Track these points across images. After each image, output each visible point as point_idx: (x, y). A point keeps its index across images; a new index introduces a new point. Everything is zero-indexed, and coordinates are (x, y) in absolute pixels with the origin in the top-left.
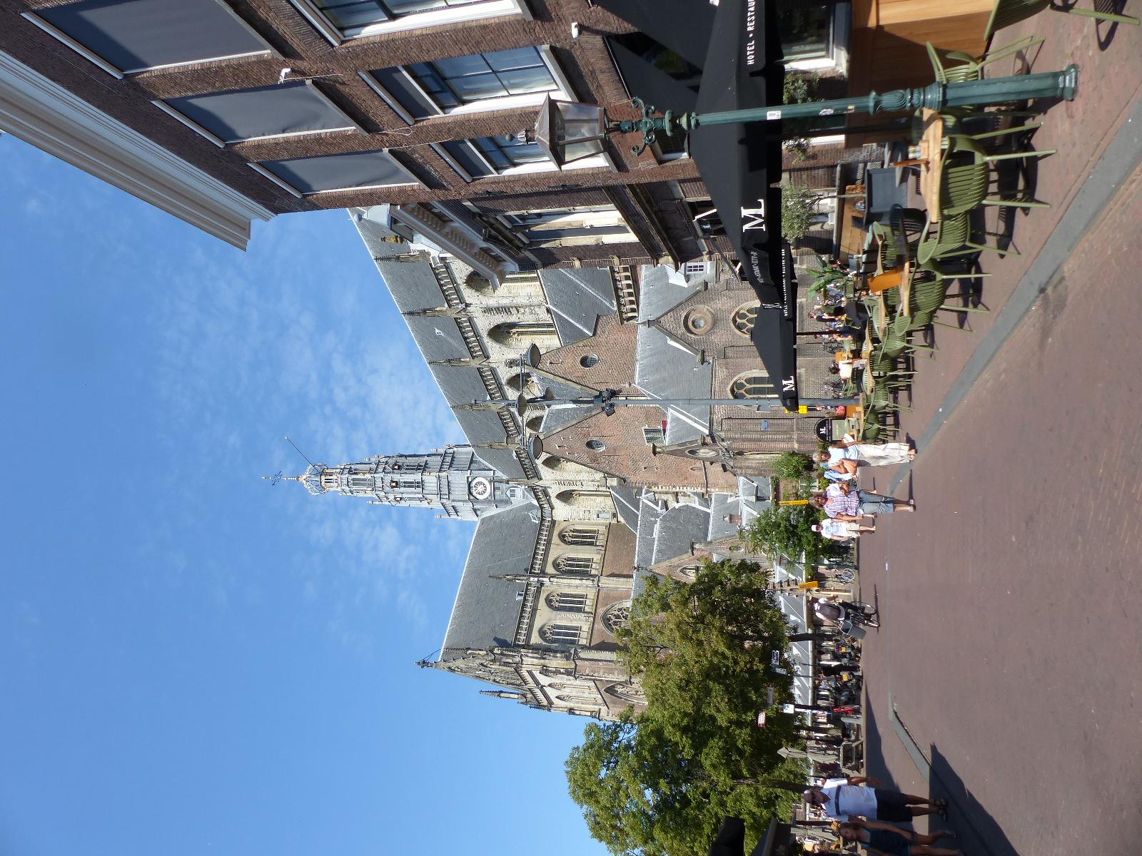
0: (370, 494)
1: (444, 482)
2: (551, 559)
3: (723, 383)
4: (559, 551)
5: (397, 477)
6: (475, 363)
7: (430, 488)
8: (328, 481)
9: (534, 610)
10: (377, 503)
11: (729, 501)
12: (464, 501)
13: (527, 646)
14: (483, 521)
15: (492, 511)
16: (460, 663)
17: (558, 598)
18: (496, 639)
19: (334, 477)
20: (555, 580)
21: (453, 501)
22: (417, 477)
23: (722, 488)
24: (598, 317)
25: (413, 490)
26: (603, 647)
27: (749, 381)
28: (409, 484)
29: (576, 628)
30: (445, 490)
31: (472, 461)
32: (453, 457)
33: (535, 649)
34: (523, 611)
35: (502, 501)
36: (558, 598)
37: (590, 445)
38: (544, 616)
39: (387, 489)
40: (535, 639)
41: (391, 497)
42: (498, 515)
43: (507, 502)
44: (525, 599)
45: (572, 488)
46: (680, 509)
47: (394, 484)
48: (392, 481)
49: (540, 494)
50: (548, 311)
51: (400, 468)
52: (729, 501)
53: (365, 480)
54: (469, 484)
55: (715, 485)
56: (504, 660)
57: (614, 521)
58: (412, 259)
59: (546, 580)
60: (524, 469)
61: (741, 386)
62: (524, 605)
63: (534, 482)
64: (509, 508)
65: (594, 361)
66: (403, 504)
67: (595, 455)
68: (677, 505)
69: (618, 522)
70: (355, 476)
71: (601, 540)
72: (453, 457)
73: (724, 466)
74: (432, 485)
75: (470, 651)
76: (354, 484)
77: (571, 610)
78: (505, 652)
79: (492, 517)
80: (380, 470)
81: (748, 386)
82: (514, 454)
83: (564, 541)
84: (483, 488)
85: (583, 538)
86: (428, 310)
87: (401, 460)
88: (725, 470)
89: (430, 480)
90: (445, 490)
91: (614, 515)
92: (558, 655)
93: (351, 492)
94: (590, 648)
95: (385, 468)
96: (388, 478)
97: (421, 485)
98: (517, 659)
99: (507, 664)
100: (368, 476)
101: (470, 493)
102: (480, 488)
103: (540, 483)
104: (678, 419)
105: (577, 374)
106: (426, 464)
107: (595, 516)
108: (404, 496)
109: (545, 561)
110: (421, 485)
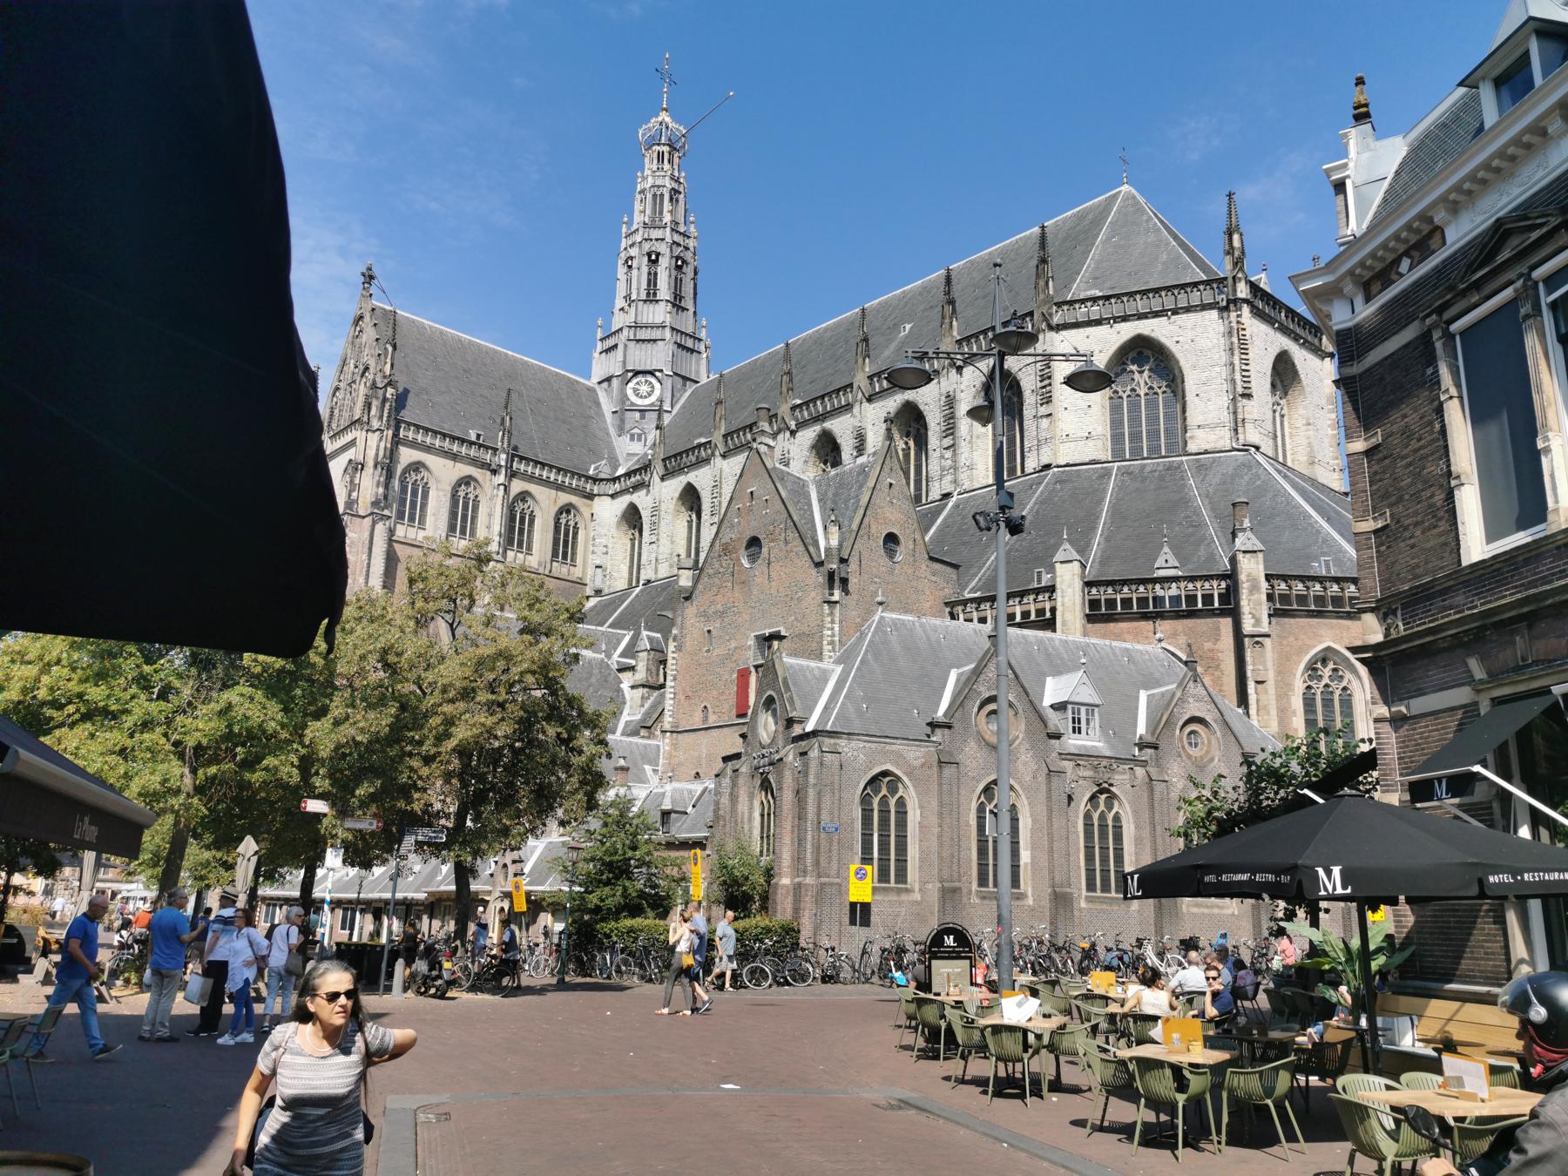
0: (638, 219)
1: (656, 334)
2: (533, 488)
3: (899, 758)
4: (546, 503)
5: (664, 262)
6: (860, 380)
8: (660, 157)
9: (455, 457)
10: (624, 229)
11: (647, 767)
12: (624, 362)
13: (397, 441)
14: (591, 390)
15: (607, 406)
16: (369, 334)
17: (471, 496)
18: (406, 392)
19: (666, 166)
20: (501, 492)
22: (664, 292)
23: (670, 756)
24: (955, 566)
26: (391, 560)
27: (901, 803)
29: (422, 521)
30: (642, 335)
31: (685, 379)
32: (692, 351)
33: (392, 454)
34: (453, 438)
35: (622, 421)
36: (471, 496)
37: (754, 542)
38: (443, 473)
39: (647, 247)
40: (407, 455)
41: (634, 252)
42: (600, 414)
43: (621, 430)
44: (472, 443)
45: (646, 527)
46: (619, 690)
48: (658, 255)
49: (639, 476)
50: (947, 496)
51: (679, 268)
52: (647, 767)
53: (661, 212)
54: (651, 373)
55: (674, 746)
56: (375, 404)
57: (589, 591)
58: (1042, 283)
59: (501, 478)
60: (680, 454)
61: (893, 789)
62: (463, 441)
63: (659, 469)
64: (612, 431)
65: (891, 553)
66: (621, 271)
67: (735, 550)
68: (625, 686)
70: (667, 198)
71: (560, 569)
72: (692, 351)
73: (737, 756)
75: (390, 349)
76: (655, 195)
77: (453, 514)
78: (387, 406)
79: (598, 404)
80: (677, 238)
81: (892, 802)
82: (703, 440)
83: (560, 512)
84: (644, 394)
85: (564, 543)
86: (954, 310)
87: (689, 270)
88: (726, 759)
89: (659, 313)
90: (642, 334)
91: (598, 592)
92: (381, 490)
93: (642, 192)
94: (390, 541)
95: (679, 245)
97: (651, 298)
98: (375, 424)
99: (368, 406)
100: (667, 218)
101: (637, 373)
102: (644, 389)
103: (656, 478)
104: (826, 681)
105: (873, 527)
106: (684, 309)
107: (598, 562)
108: (635, 272)
109: (532, 479)
110: (651, 298)
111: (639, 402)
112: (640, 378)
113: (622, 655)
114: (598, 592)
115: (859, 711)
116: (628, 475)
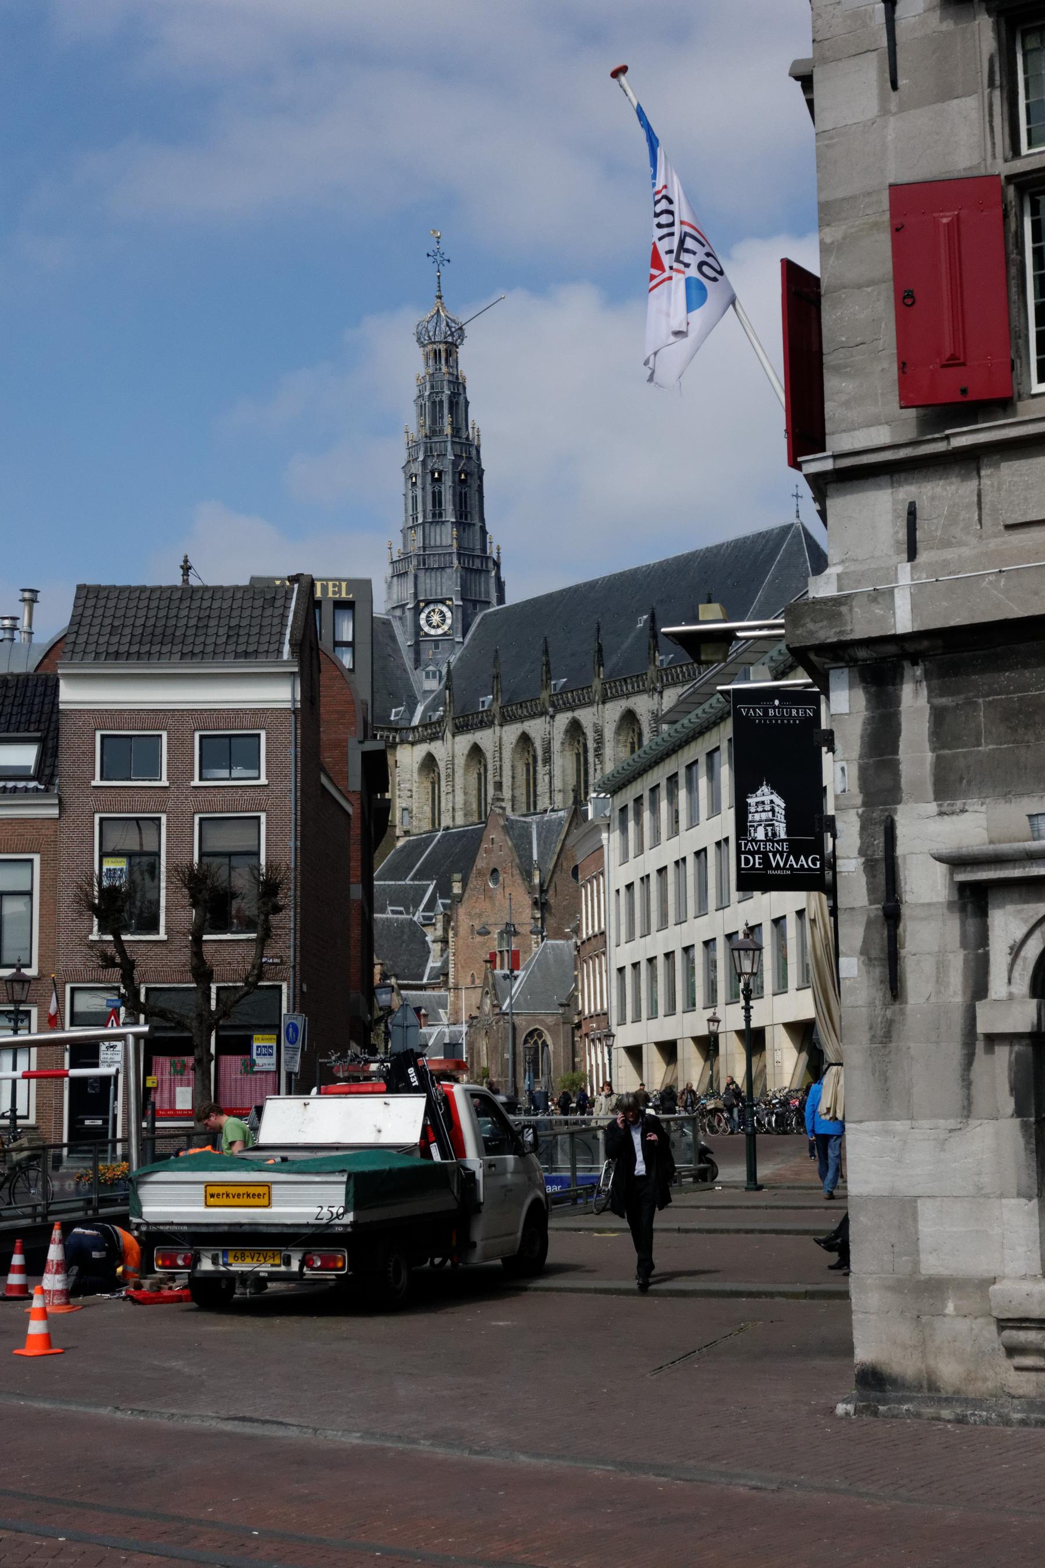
7: (433, 535)
15: (404, 640)
21: (416, 577)
25: (430, 507)
28: (437, 499)
31: (475, 602)
46: (425, 942)
47: (436, 475)
52: (440, 1011)
69: (398, 837)
72: (479, 571)
74: (438, 538)
79: (393, 638)
81: (540, 1042)
91: (407, 833)
96: (448, 468)
100: (448, 430)
102: (436, 618)
107: (404, 805)
111: (433, 632)
112: (432, 607)
113: (423, 911)
114: (407, 833)
115: (526, 1000)
116: (425, 726)
